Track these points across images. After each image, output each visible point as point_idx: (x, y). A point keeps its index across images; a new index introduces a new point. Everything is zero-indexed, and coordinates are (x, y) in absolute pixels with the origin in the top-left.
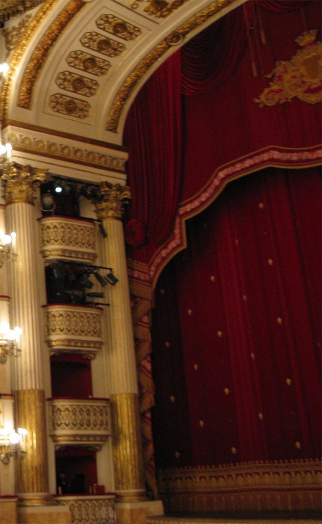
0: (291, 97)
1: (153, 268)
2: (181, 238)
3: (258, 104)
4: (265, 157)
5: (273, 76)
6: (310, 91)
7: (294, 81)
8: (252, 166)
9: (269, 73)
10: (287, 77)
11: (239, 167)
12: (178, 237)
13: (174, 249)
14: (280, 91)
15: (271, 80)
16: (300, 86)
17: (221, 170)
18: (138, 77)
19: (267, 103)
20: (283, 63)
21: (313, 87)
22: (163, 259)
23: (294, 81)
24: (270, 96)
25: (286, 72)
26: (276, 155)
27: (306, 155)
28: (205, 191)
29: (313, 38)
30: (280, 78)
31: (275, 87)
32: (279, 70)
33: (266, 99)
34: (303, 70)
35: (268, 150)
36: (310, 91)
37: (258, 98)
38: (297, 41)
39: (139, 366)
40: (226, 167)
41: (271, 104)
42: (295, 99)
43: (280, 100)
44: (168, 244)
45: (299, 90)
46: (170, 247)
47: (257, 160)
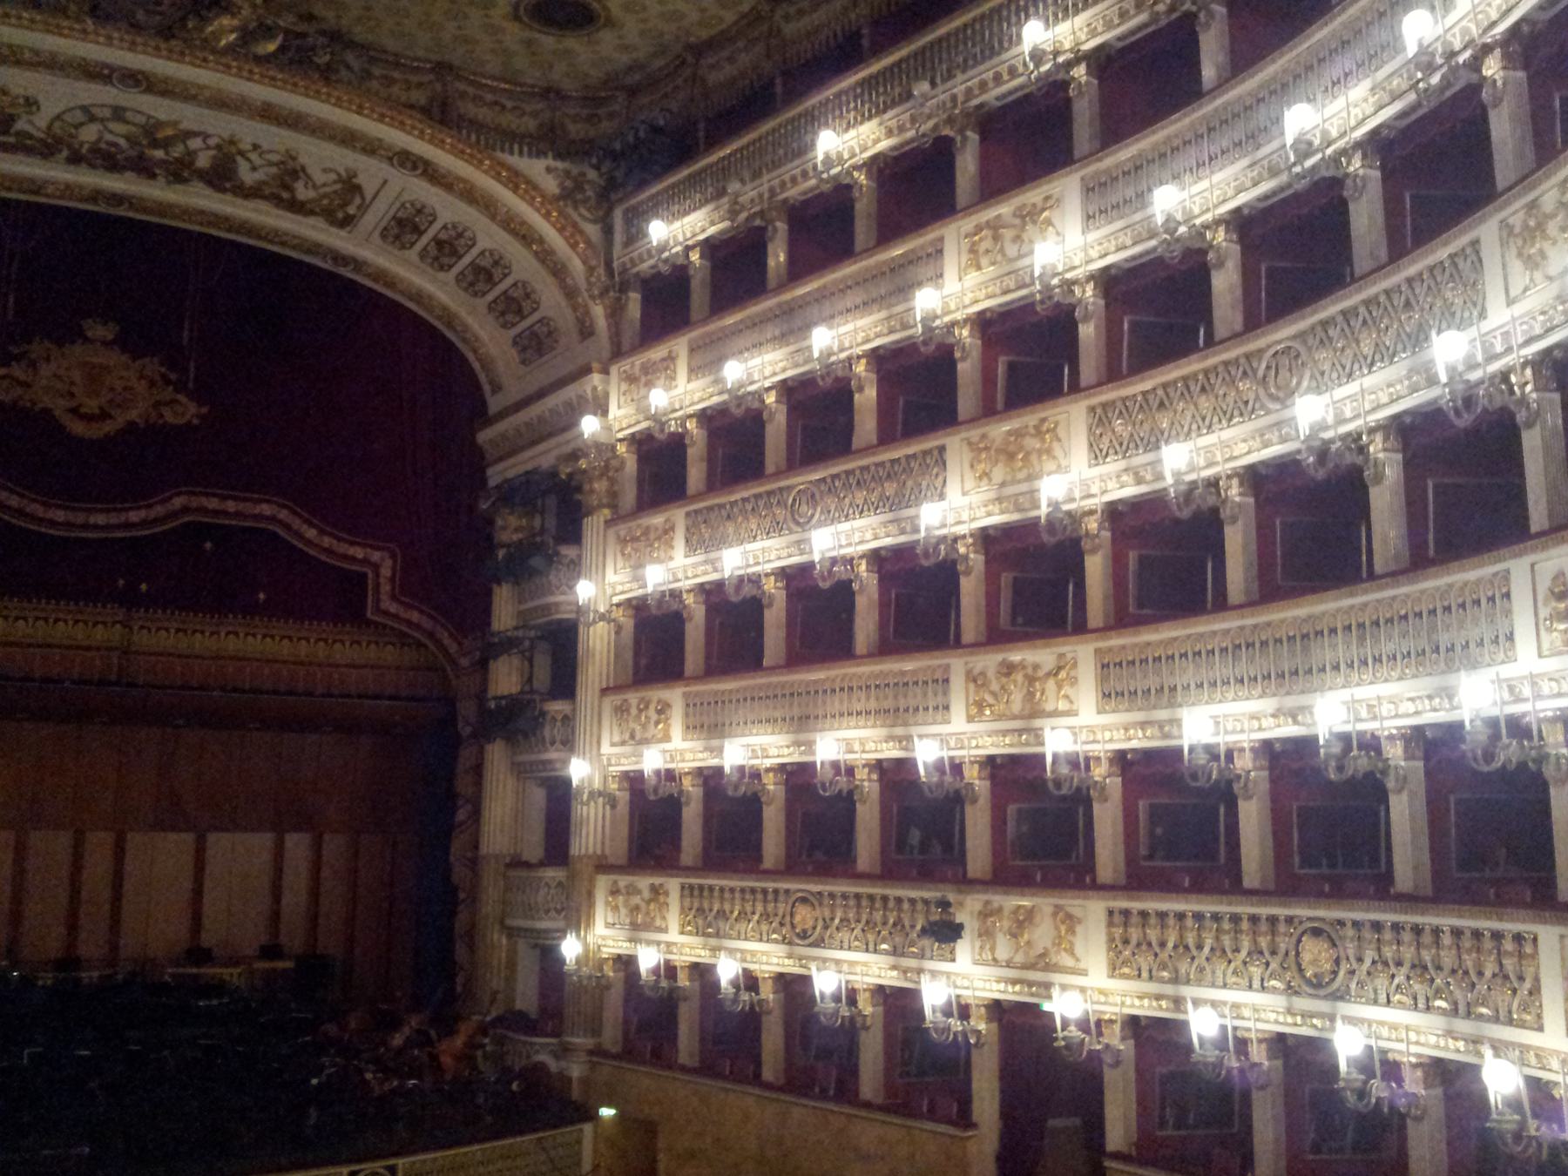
0: (40, 406)
5: (24, 354)
6: (74, 411)
10: (46, 371)
15: (18, 358)
21: (83, 410)
23: (59, 385)
25: (48, 359)
27: (37, 509)
29: (110, 337)
30: (33, 365)
31: (18, 371)
32: (37, 348)
34: (77, 375)
42: (47, 412)
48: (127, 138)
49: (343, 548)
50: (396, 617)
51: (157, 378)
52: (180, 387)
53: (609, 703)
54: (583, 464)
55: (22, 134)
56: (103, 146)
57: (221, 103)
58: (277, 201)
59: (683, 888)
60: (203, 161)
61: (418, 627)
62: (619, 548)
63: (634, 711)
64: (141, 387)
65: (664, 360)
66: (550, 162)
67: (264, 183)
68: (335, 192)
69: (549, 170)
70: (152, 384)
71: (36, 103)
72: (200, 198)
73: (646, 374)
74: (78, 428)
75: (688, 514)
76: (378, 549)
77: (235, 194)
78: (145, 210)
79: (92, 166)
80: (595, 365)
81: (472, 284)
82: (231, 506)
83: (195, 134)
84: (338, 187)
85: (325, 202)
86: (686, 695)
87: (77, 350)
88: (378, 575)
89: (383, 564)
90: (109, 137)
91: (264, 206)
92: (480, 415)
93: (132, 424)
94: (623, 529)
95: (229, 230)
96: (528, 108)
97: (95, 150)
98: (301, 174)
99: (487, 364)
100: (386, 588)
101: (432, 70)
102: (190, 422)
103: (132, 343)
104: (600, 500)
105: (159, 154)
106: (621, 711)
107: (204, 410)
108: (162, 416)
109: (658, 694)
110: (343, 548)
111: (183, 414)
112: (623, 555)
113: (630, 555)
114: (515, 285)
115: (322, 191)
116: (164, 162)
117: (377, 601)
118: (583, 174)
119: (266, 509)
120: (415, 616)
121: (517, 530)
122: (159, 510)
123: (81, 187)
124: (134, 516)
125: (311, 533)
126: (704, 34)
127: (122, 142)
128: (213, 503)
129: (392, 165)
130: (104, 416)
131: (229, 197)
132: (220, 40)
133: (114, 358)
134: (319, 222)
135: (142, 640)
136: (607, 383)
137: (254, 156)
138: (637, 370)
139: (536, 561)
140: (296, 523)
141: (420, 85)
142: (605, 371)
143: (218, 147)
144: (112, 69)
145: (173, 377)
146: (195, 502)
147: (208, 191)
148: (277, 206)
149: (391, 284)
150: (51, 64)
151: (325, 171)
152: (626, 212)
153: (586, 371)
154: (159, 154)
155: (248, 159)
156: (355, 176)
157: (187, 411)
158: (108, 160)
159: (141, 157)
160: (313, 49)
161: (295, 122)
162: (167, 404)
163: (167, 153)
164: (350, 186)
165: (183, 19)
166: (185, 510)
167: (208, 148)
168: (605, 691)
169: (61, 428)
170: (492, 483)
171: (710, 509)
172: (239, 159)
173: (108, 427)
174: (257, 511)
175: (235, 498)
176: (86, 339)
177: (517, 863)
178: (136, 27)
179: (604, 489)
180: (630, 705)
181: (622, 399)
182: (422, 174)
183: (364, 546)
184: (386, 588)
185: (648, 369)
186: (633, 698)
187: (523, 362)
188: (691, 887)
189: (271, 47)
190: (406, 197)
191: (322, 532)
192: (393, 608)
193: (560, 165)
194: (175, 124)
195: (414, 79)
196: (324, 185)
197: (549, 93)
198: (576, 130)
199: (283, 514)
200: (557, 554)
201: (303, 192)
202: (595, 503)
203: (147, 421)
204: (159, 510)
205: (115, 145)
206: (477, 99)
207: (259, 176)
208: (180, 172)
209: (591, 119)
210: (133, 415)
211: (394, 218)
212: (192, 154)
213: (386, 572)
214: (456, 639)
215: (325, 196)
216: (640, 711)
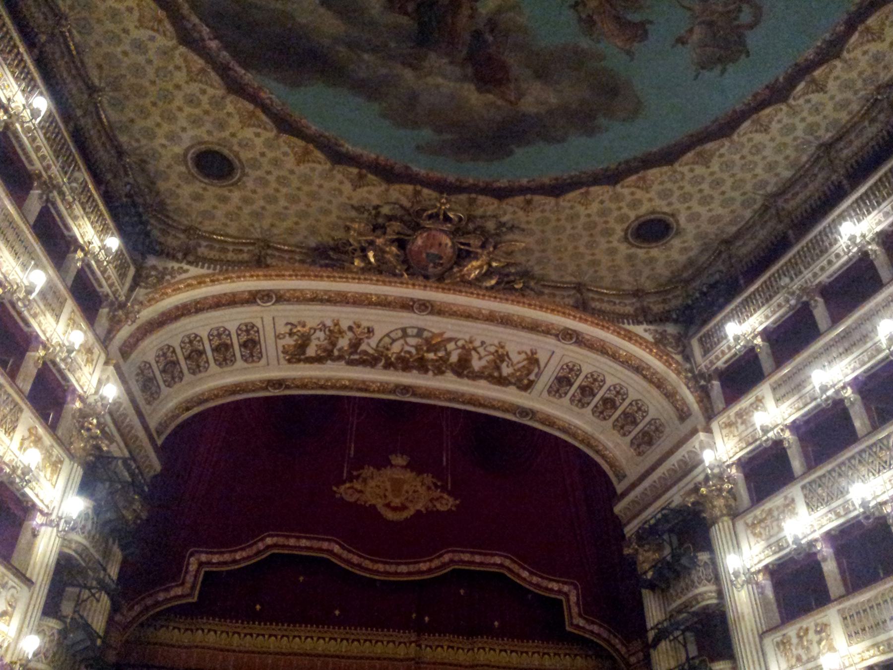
1: (138, 608)
2: (193, 588)
3: (335, 492)
4: (325, 545)
6: (388, 505)
7: (377, 491)
8: (307, 548)
9: (356, 470)
10: (372, 483)
11: (292, 542)
12: (188, 585)
14: (361, 492)
15: (358, 477)
16: (381, 497)
18: (217, 396)
19: (344, 496)
20: (372, 468)
21: (393, 504)
22: (157, 604)
23: (377, 491)
24: (350, 491)
25: (372, 478)
26: (336, 548)
27: (367, 564)
28: (243, 549)
29: (405, 463)
30: (365, 481)
32: (368, 471)
33: (344, 491)
34: (388, 485)
38: (390, 457)
40: (277, 536)
42: (373, 507)
43: (358, 499)
45: (379, 500)
46: (172, 594)
47: (316, 544)
49: (545, 583)
50: (583, 628)
51: (431, 485)
52: (444, 489)
53: (769, 642)
55: (365, 353)
56: (403, 354)
57: (468, 315)
58: (491, 379)
60: (454, 358)
61: (598, 635)
62: (749, 532)
63: (795, 640)
64: (422, 490)
66: (645, 326)
67: (485, 367)
68: (524, 367)
69: (646, 331)
70: (429, 488)
71: (373, 331)
72: (449, 383)
74: (390, 515)
75: (803, 487)
77: (468, 377)
79: (396, 369)
81: (602, 413)
82: (478, 559)
83: (450, 340)
84: (525, 363)
85: (518, 374)
87: (388, 472)
88: (568, 601)
90: (407, 348)
91: (483, 383)
92: (613, 496)
94: (749, 518)
95: (463, 403)
96: (627, 302)
98: (506, 358)
100: (575, 610)
101: (575, 288)
102: (451, 509)
104: (721, 511)
105: (431, 356)
106: (783, 645)
107: (458, 502)
108: (435, 506)
110: (545, 583)
112: (755, 534)
113: (761, 534)
114: (631, 404)
115: (516, 367)
116: (432, 360)
117: (571, 617)
118: (665, 331)
119: (498, 560)
120: (595, 629)
122: (436, 563)
123: (387, 383)
124: (424, 566)
125: (525, 574)
126: (733, 229)
127: (413, 351)
128: (466, 557)
129: (559, 340)
130: (404, 508)
131: (466, 380)
132: (471, 274)
133: (409, 475)
134: (512, 389)
135: (428, 654)
137: (481, 350)
140: (516, 568)
141: (569, 296)
143: (463, 347)
145: (439, 484)
147: (455, 378)
148: (490, 382)
149: (552, 424)
150: (384, 303)
151: (519, 353)
152: (700, 340)
153: (694, 432)
154: (431, 356)
155: (478, 353)
156: (536, 353)
157: (447, 503)
158: (404, 364)
160: (513, 281)
161: (506, 321)
162: (437, 499)
163: (435, 354)
164: (533, 360)
165: (452, 268)
166: (452, 561)
168: (762, 636)
169: (379, 515)
171: (820, 478)
172: (473, 353)
173: (406, 514)
174: (492, 561)
175: (480, 554)
178: (426, 277)
179: (722, 504)
180: (790, 637)
182: (575, 342)
183: (558, 582)
184: (575, 610)
186: (791, 631)
189: (493, 282)
190: (566, 360)
191: (531, 573)
192: (582, 623)
193: (652, 327)
194: (441, 334)
195: (565, 293)
196: (519, 363)
197: (638, 293)
198: (657, 308)
199: (507, 563)
200: (697, 557)
201: (506, 370)
202: (719, 514)
203: (426, 509)
204: (436, 563)
205: (409, 352)
206: (602, 301)
207: (483, 363)
209: (664, 301)
210: (420, 506)
211: (556, 378)
212: (449, 354)
213: (573, 598)
214: (623, 644)
215: (519, 370)
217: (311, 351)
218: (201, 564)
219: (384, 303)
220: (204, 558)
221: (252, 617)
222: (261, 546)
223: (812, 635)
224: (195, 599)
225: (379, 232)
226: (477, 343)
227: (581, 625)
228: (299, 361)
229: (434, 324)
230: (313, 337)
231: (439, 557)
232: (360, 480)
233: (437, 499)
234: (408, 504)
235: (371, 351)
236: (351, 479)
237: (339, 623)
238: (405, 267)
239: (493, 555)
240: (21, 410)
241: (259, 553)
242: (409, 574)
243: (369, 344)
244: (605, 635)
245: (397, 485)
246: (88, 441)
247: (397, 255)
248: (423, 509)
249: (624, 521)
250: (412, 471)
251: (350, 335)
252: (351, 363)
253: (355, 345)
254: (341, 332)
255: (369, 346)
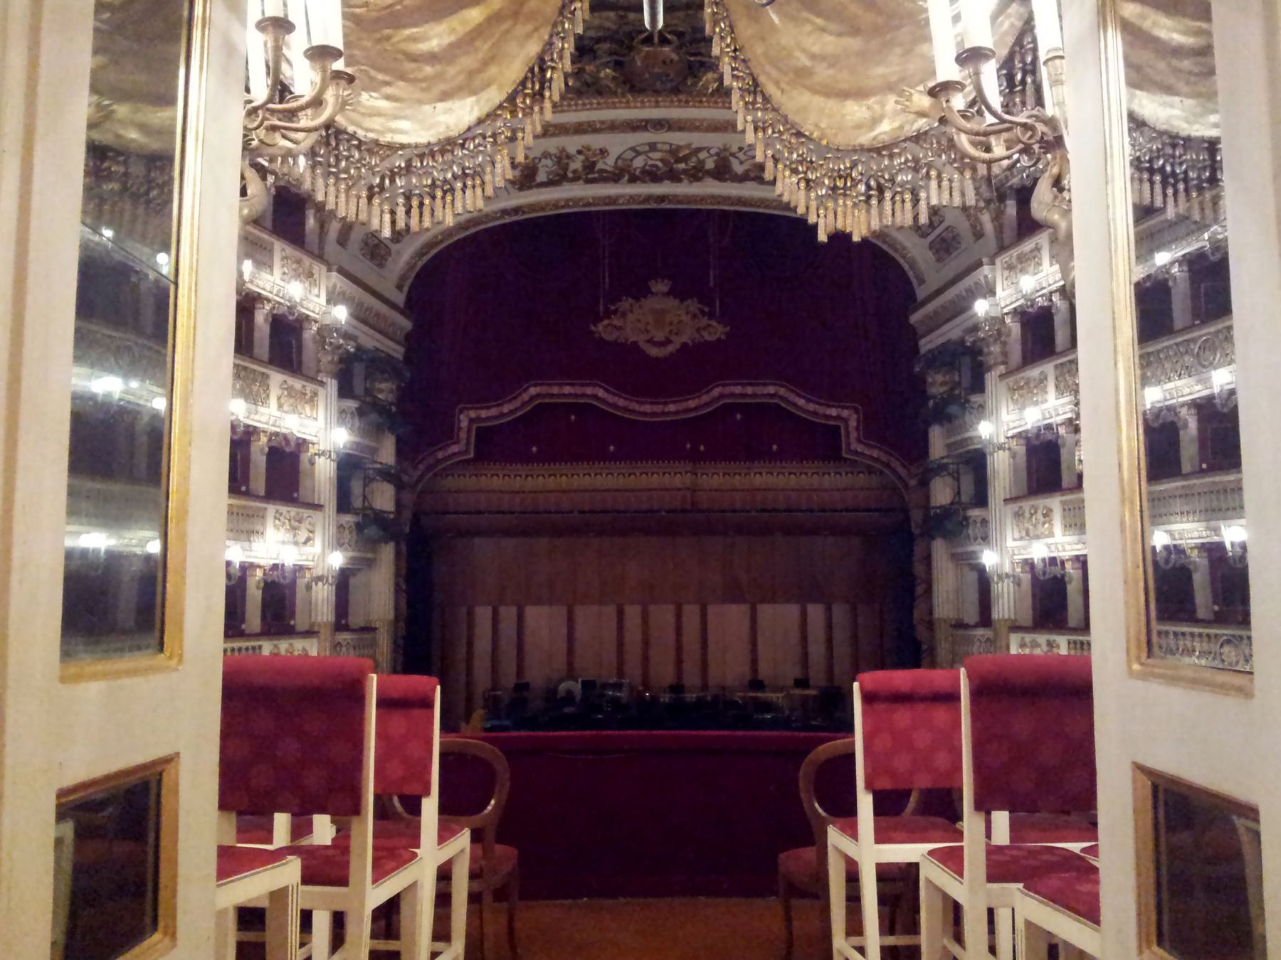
0: (631, 340)
1: (421, 467)
2: (468, 443)
3: (592, 333)
4: (589, 391)
5: (617, 310)
6: (650, 341)
9: (613, 303)
10: (630, 317)
11: (555, 390)
12: (464, 442)
13: (455, 454)
17: (535, 385)
20: (630, 300)
21: (655, 340)
22: (439, 461)
25: (631, 311)
26: (601, 393)
29: (666, 289)
30: (624, 315)
31: (617, 321)
32: (625, 304)
33: (602, 329)
35: (594, 385)
36: (650, 341)
37: (595, 325)
39: (397, 585)
40: (542, 385)
41: (607, 337)
42: (635, 343)
43: (619, 337)
44: (448, 446)
47: (578, 390)
48: (662, 160)
49: (821, 410)
51: (697, 312)
52: (711, 315)
54: (981, 335)
55: (602, 171)
56: (647, 168)
59: (1069, 643)
60: (710, 165)
61: (877, 460)
63: (1027, 515)
64: (685, 318)
65: (1032, 251)
70: (695, 316)
71: (606, 151)
73: (1021, 262)
74: (654, 352)
75: (1056, 367)
76: (847, 408)
77: (733, 181)
78: (679, 202)
79: (644, 182)
80: (985, 260)
82: (749, 390)
83: (699, 150)
86: (1063, 503)
87: (650, 303)
89: (852, 419)
90: (650, 162)
92: (910, 300)
93: (684, 345)
94: (1011, 380)
95: (732, 204)
97: (644, 171)
99: (913, 264)
100: (854, 435)
103: (677, 293)
105: (682, 166)
109: (1042, 502)
111: (716, 333)
112: (1013, 400)
117: (849, 444)
119: (771, 390)
120: (875, 453)
121: (943, 384)
122: (705, 398)
123: (639, 196)
125: (801, 402)
127: (660, 164)
128: (738, 390)
130: (668, 342)
131: (728, 184)
132: (708, 89)
133: (672, 303)
136: (994, 271)
137: (741, 155)
138: (1014, 260)
139: (953, 409)
142: (993, 263)
143: (717, 154)
144: (647, 121)
145: (706, 309)
146: (728, 390)
147: (717, 183)
150: (613, 127)
153: (979, 264)
154: (682, 166)
155: (737, 158)
157: (717, 331)
158: (652, 176)
159: (671, 170)
162: (705, 328)
165: (685, 79)
166: (722, 396)
167: (711, 156)
170: (923, 351)
172: (732, 159)
173: (670, 349)
174: (765, 392)
175: (751, 384)
176: (652, 293)
177: (960, 625)
178: (657, 92)
181: (1005, 282)
184: (854, 435)
185: (1022, 259)
186: (1026, 505)
187: (938, 260)
188: (1075, 642)
192: (860, 448)
194: (689, 146)
199: (782, 391)
200: (968, 401)
203: (693, 341)
204: (705, 398)
205: (652, 166)
208: (697, 174)
210: (685, 339)
212: (702, 162)
213: (853, 423)
214: (904, 466)
216: (1032, 515)
217: (541, 177)
218: (471, 421)
219: (613, 127)
220: (473, 414)
221: (527, 459)
222: (526, 397)
223: (1040, 516)
224: (472, 455)
225: (586, 58)
226: (734, 149)
227: (859, 450)
228: (530, 188)
229: (678, 138)
230: (540, 165)
231: (708, 392)
232: (619, 314)
233: (705, 328)
234: (673, 338)
235: (609, 169)
236: (608, 314)
237: (614, 458)
238: (628, 86)
239: (765, 385)
240: (267, 377)
241: (524, 404)
242: (677, 412)
243: (606, 164)
244: (884, 458)
245: (660, 314)
246: (334, 353)
247: (614, 78)
248: (689, 342)
249: (920, 332)
250: (675, 298)
251: (581, 158)
252: (588, 181)
253: (590, 166)
254: (569, 157)
255: (608, 163)
